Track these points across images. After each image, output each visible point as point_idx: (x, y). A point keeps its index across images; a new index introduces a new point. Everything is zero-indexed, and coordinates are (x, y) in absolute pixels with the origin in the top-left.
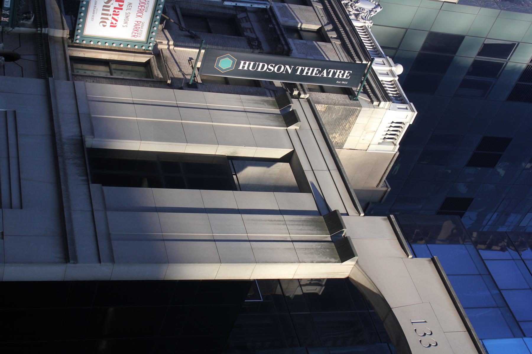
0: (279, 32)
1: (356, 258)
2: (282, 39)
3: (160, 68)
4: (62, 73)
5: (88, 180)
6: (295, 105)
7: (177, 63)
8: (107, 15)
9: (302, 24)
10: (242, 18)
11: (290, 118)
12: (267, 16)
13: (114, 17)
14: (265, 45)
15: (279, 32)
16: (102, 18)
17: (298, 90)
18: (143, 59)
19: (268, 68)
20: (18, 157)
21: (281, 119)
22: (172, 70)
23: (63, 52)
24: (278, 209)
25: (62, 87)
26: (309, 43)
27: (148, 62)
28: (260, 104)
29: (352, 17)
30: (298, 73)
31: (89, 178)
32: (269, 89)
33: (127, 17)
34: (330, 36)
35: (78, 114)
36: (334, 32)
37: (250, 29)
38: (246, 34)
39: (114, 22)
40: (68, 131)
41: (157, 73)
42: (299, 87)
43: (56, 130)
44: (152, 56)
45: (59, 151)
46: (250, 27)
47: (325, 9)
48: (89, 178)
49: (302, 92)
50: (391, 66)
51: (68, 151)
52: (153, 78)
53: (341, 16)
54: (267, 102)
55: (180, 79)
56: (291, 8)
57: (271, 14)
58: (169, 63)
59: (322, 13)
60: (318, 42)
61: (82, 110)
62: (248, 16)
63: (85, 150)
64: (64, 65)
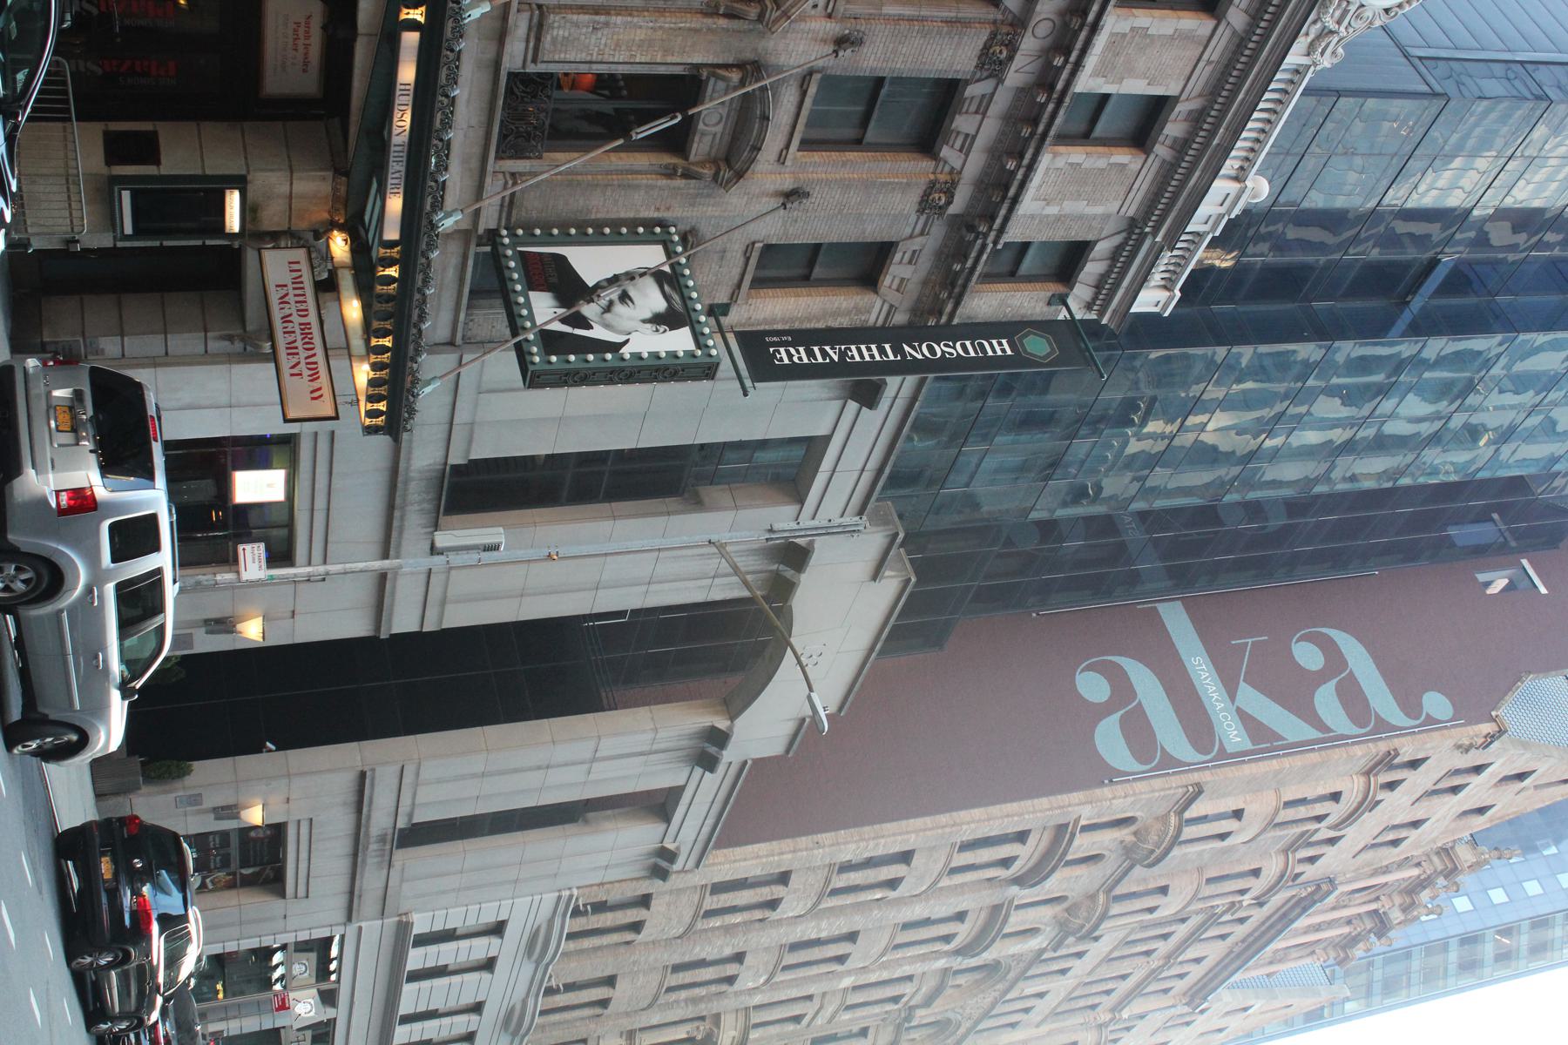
2: (1003, 212)
29: (1301, 44)
37: (967, 135)
46: (972, 132)
47: (1240, 42)
53: (1241, 96)
57: (1041, 128)
62: (993, 94)
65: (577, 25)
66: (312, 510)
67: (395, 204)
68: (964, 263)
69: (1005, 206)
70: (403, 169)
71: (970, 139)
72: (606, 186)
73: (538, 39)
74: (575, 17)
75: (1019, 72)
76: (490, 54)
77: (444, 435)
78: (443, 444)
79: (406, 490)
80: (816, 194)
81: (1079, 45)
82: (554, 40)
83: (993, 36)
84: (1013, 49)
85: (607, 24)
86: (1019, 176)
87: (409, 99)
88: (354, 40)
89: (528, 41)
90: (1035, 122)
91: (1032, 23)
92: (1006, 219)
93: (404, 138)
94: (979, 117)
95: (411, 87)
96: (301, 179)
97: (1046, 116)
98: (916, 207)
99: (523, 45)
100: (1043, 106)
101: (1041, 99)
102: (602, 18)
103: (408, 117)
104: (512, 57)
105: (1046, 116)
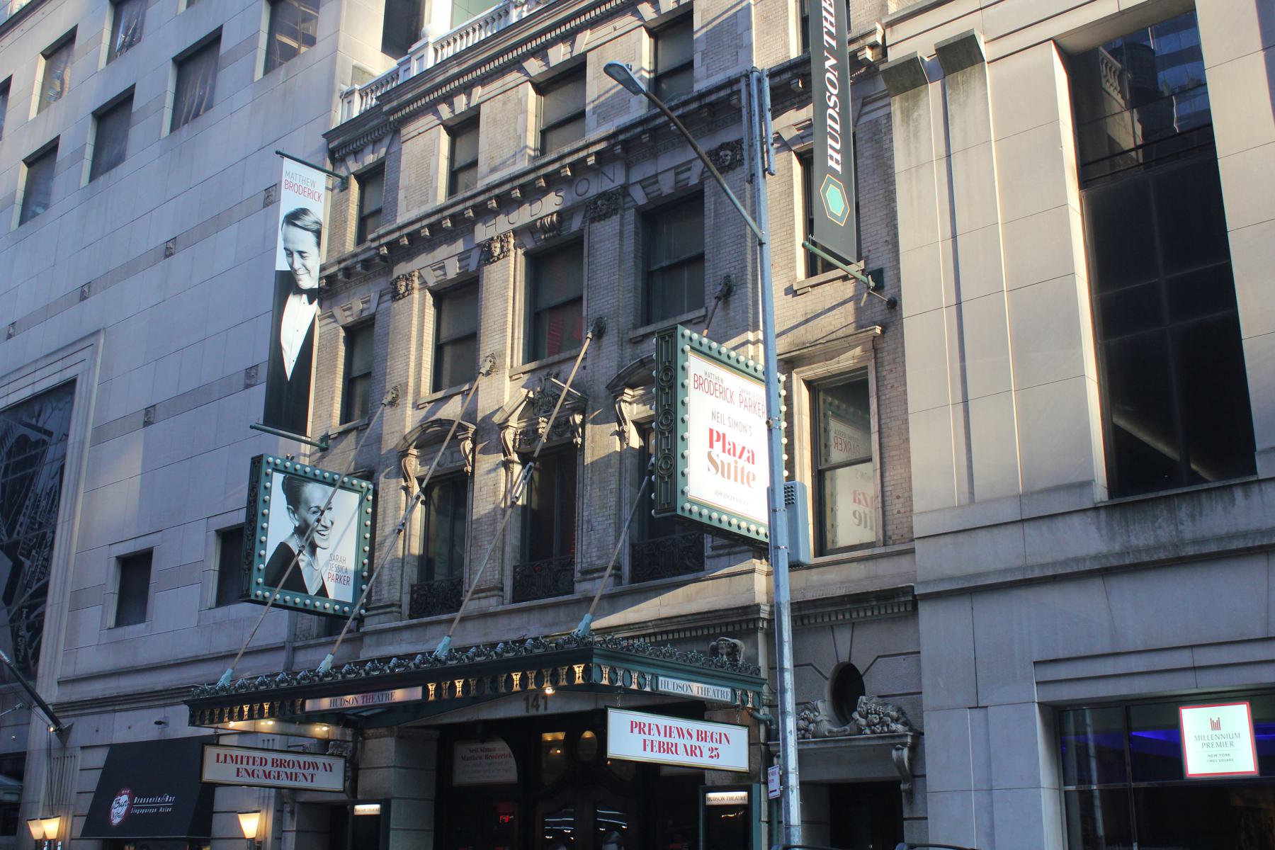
0: (695, 105)
1: (976, 33)
2: (713, 97)
3: (829, 356)
4: (903, 564)
5: (1245, 485)
6: (924, 48)
7: (807, 321)
8: (736, 468)
9: (642, 69)
10: (647, 195)
11: (960, 56)
12: (645, 138)
13: (738, 452)
14: (729, 136)
15: (695, 105)
16: (736, 480)
17: (862, 49)
18: (802, 397)
19: (833, 108)
20: (1192, 647)
21: (959, 76)
22: (832, 328)
23: (814, 570)
24: (1262, 54)
25: (930, 566)
26: (700, 47)
27: (809, 384)
28: (916, 127)
30: (834, 43)
31: (1238, 481)
32: (860, 116)
33: (736, 424)
34: (464, 108)
35: (1022, 521)
36: (456, 100)
37: (677, 174)
38: (694, 181)
39: (746, 455)
40: (1086, 541)
41: (847, 361)
42: (855, 47)
43: (1088, 566)
44: (794, 376)
45: (1162, 555)
46: (672, 173)
47: (593, 24)
48: (1238, 481)
49: (870, 40)
50: (426, 45)
51: (1150, 533)
52: (866, 368)
54: (907, 114)
55: (858, 310)
56: (599, 97)
57: (639, 129)
58: (811, 338)
59: (605, 31)
60: (695, 28)
61: (1010, 513)
62: (640, 182)
63: (1116, 501)
64: (855, 564)
65: (589, 544)
66: (1194, 668)
67: (399, 695)
68: (790, 79)
69: (708, 100)
71: (678, 170)
75: (614, 179)
77: (1044, 526)
78: (1060, 522)
79: (1148, 549)
80: (723, 273)
81: (575, 157)
82: (599, 558)
83: (593, 220)
84: (600, 196)
85: (589, 521)
86: (680, 111)
89: (594, 579)
90: (639, 136)
91: (579, 198)
92: (718, 88)
93: (359, 697)
94: (660, 178)
97: (629, 135)
98: (738, 169)
99: (598, 581)
100: (624, 142)
101: (618, 149)
103: (348, 697)
105: (629, 135)
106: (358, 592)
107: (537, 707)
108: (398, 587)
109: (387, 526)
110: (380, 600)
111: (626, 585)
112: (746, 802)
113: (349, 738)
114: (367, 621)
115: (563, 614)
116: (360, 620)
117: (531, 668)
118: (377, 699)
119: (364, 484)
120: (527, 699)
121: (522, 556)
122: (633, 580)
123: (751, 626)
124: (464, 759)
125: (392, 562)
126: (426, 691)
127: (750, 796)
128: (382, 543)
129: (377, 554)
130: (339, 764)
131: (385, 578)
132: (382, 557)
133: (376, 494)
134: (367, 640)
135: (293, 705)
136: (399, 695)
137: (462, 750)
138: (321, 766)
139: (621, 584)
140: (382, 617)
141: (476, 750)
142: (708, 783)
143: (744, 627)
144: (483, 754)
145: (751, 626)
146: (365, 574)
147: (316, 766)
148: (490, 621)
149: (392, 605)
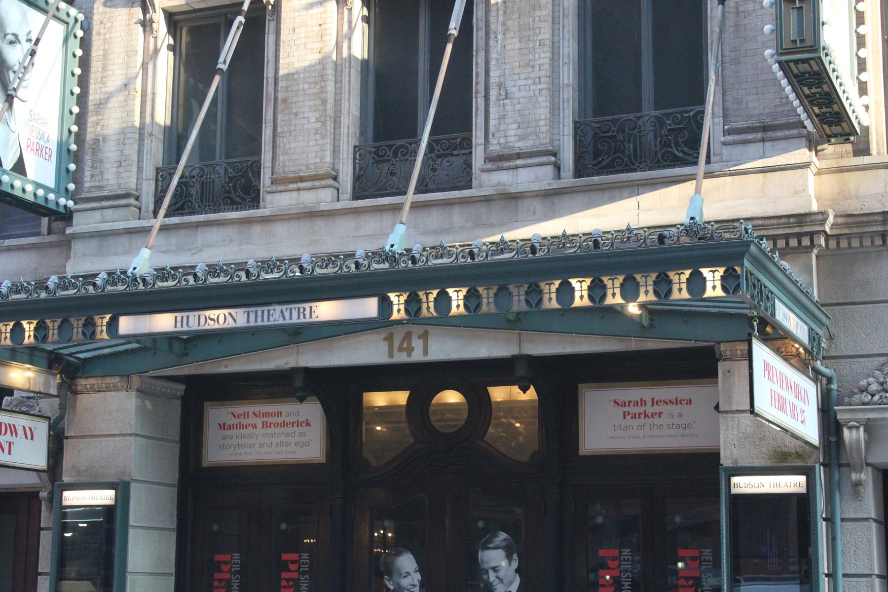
65: (502, 118)
67: (326, 310)
70: (278, 308)
72: (737, 12)
73: (519, 156)
74: (493, 123)
76: (537, 204)
82: (521, 138)
87: (193, 316)
88: (530, 356)
89: (517, 167)
95: (179, 315)
96: (729, 399)
99: (520, 170)
102: (493, 93)
104: (537, 180)
106: (62, 172)
107: (410, 350)
108: (134, 169)
109: (109, 77)
110: (101, 188)
111: (568, 179)
112: (803, 490)
113: (54, 391)
114: (76, 218)
115: (457, 216)
116: (67, 216)
117: (613, 270)
118: (278, 315)
119: (73, 12)
120: (389, 339)
121: (362, 133)
122: (579, 172)
123: (806, 242)
124: (222, 427)
125: (123, 132)
126: (385, 305)
127: (810, 484)
128: (101, 104)
129: (91, 119)
130: (42, 429)
131: (110, 153)
132: (110, 122)
133: (87, 28)
134: (78, 247)
135: (90, 324)
136: (326, 310)
137: (217, 415)
138: (20, 431)
139: (559, 177)
140: (109, 213)
141: (246, 415)
142: (726, 461)
143: (794, 243)
144: (259, 421)
145: (806, 242)
146: (74, 147)
147: (13, 430)
148: (319, 223)
149: (127, 196)
